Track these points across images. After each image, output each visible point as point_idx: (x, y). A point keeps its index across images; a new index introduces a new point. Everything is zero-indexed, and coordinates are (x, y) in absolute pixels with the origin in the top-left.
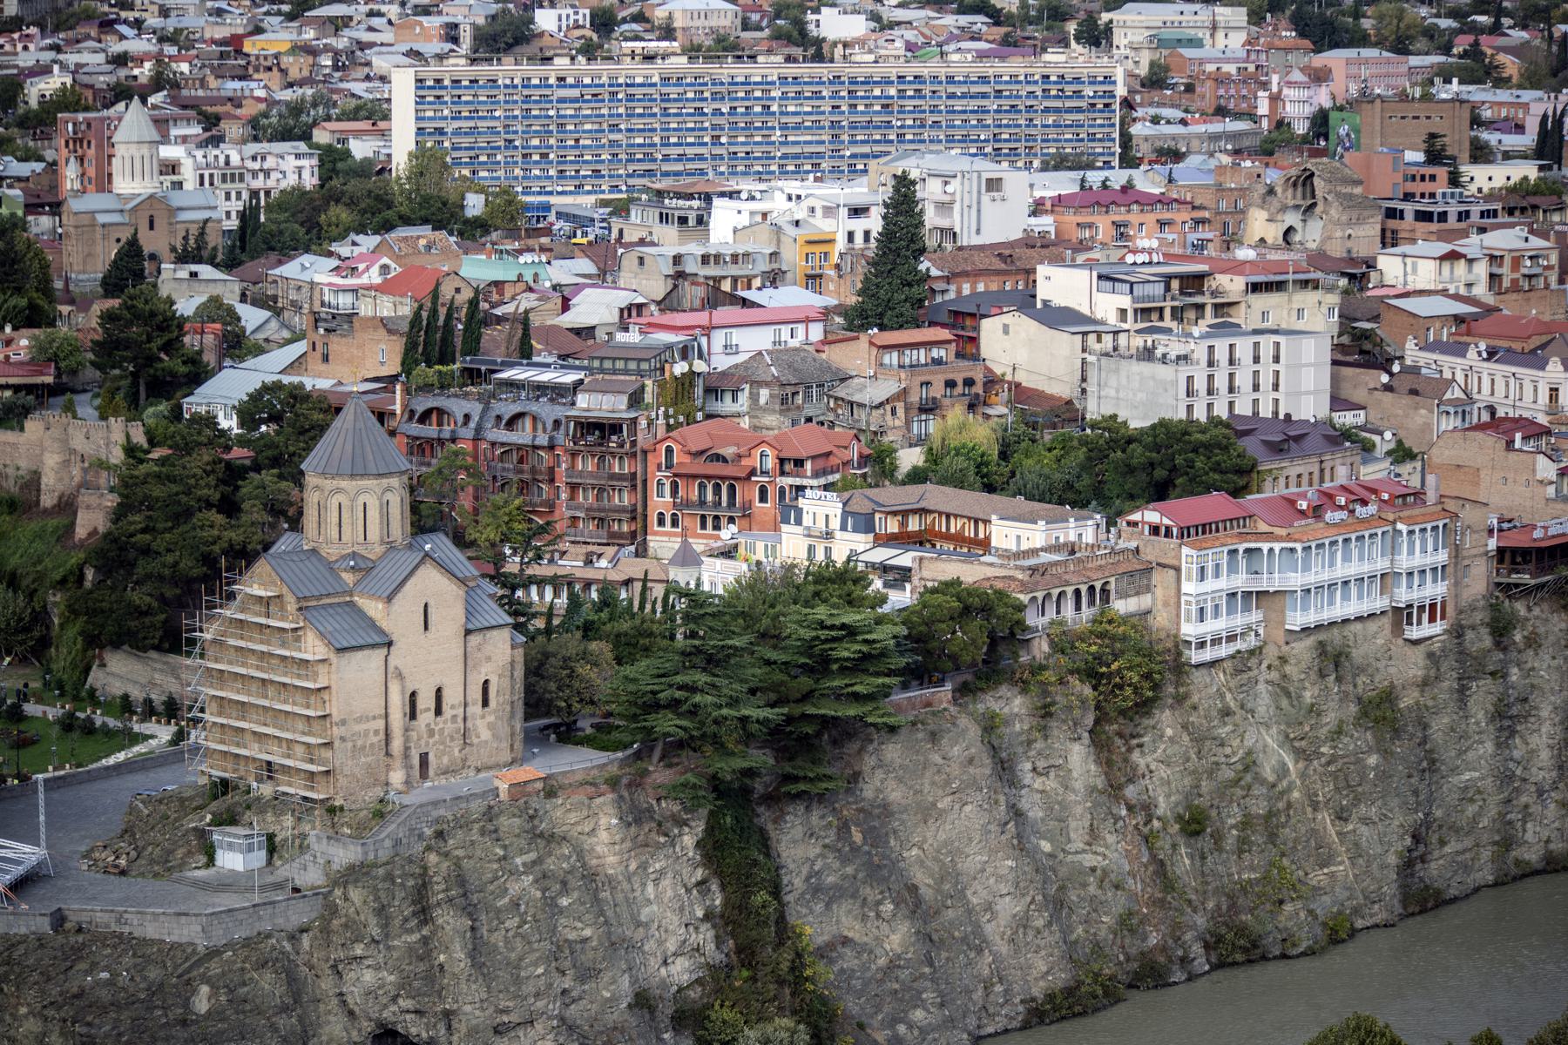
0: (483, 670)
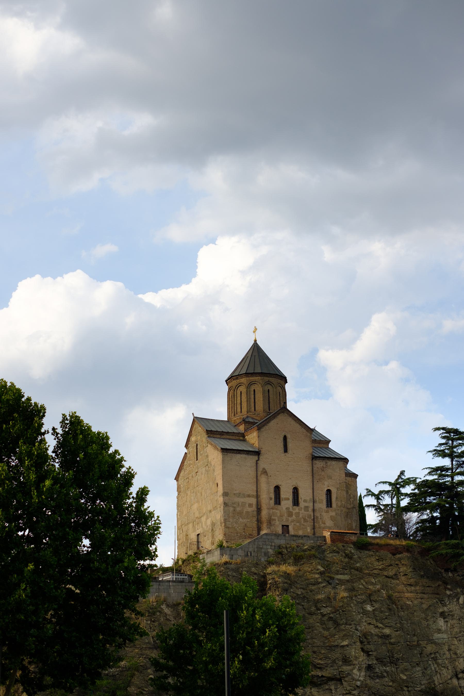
0: (326, 483)
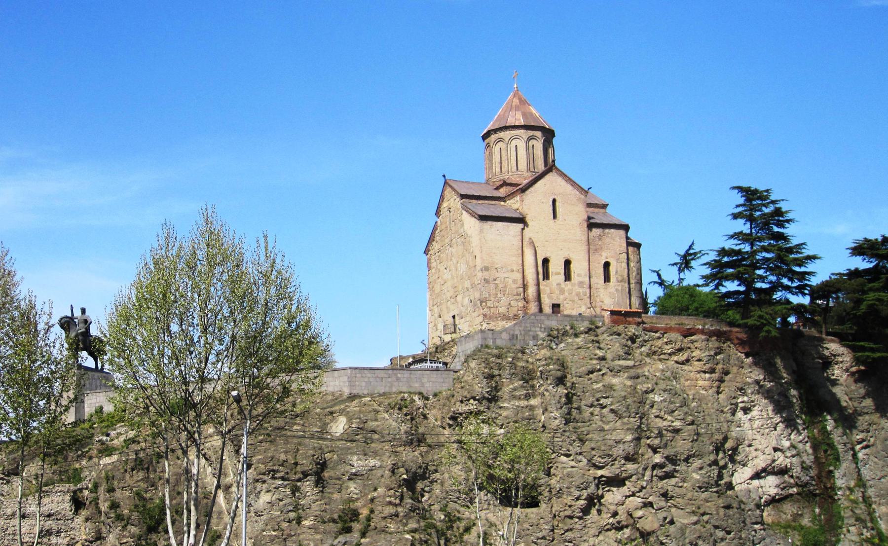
0: (604, 254)
